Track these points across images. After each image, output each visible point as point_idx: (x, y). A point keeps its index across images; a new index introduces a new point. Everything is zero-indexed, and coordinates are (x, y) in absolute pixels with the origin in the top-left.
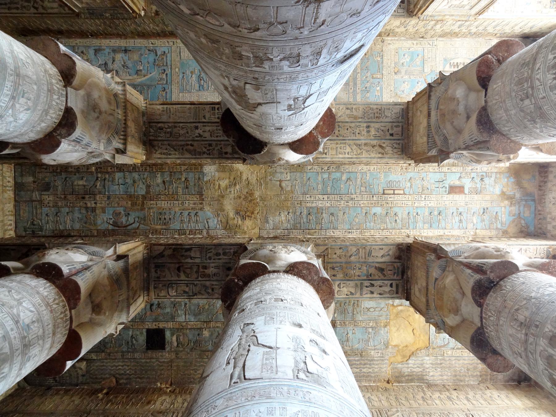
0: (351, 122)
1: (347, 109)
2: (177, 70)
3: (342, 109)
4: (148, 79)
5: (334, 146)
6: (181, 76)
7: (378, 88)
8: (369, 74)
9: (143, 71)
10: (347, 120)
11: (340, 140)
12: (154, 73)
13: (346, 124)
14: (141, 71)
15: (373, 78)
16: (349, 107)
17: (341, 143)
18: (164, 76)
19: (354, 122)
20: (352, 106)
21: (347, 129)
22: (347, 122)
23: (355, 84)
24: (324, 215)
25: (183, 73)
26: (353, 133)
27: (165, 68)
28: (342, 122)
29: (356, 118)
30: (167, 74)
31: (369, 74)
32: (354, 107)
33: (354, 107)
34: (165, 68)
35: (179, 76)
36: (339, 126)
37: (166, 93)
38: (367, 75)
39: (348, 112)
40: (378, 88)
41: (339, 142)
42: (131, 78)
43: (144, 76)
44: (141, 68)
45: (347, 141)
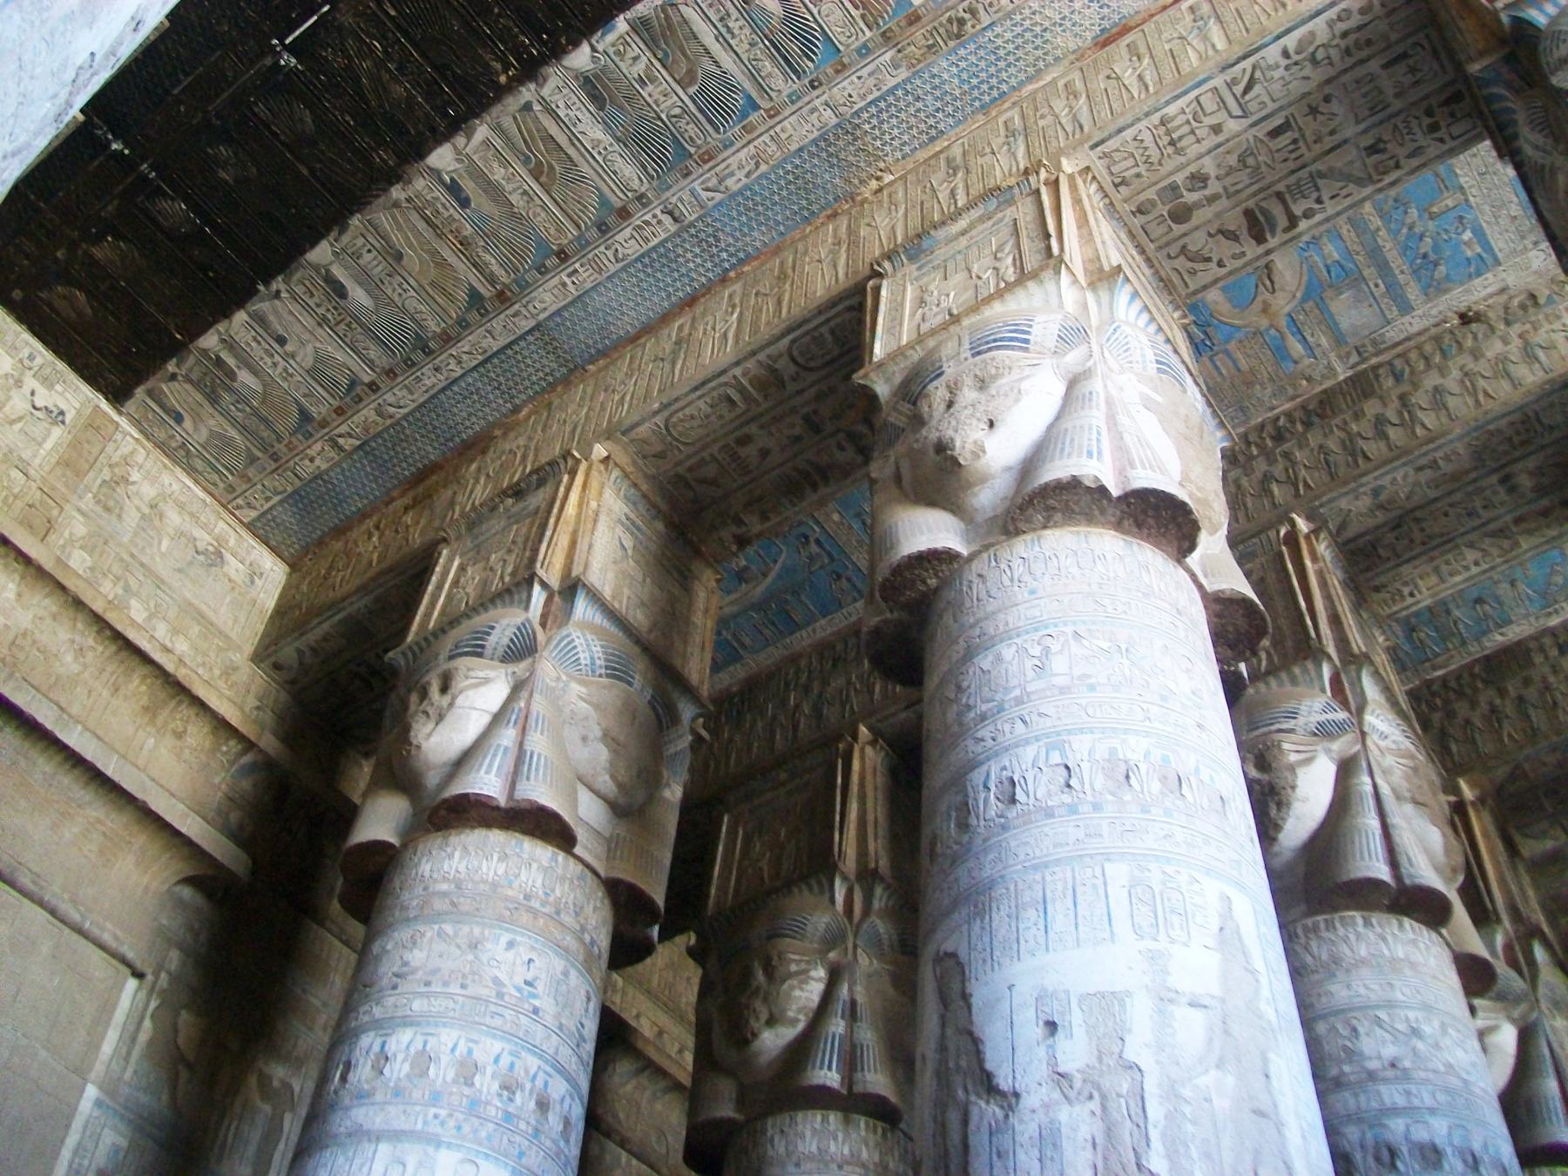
0: (1450, 493)
1: (1420, 469)
2: (836, 517)
3: (1405, 477)
4: (779, 576)
5: (1428, 568)
6: (856, 526)
7: (1467, 235)
8: (1414, 212)
9: (753, 567)
10: (1432, 494)
11: (1434, 548)
12: (784, 555)
13: (1439, 505)
14: (746, 568)
15: (1432, 217)
16: (1423, 461)
17: (1442, 554)
18: (814, 548)
19: (1459, 489)
20: (1430, 457)
21: (1446, 515)
22: (1436, 500)
23: (1384, 268)
24: (1456, 613)
25: (858, 515)
26: (1469, 515)
27: (802, 529)
28: (1420, 507)
29: (1454, 477)
30: (818, 542)
31: (1414, 212)
32: (1439, 454)
33: (1439, 454)
34: (802, 529)
35: (850, 527)
36: (1417, 520)
37: (849, 580)
38: (1409, 221)
39: (1428, 474)
40: (1467, 235)
41: (1436, 553)
42: (733, 596)
43: (765, 575)
44: (744, 563)
45: (1459, 541)
